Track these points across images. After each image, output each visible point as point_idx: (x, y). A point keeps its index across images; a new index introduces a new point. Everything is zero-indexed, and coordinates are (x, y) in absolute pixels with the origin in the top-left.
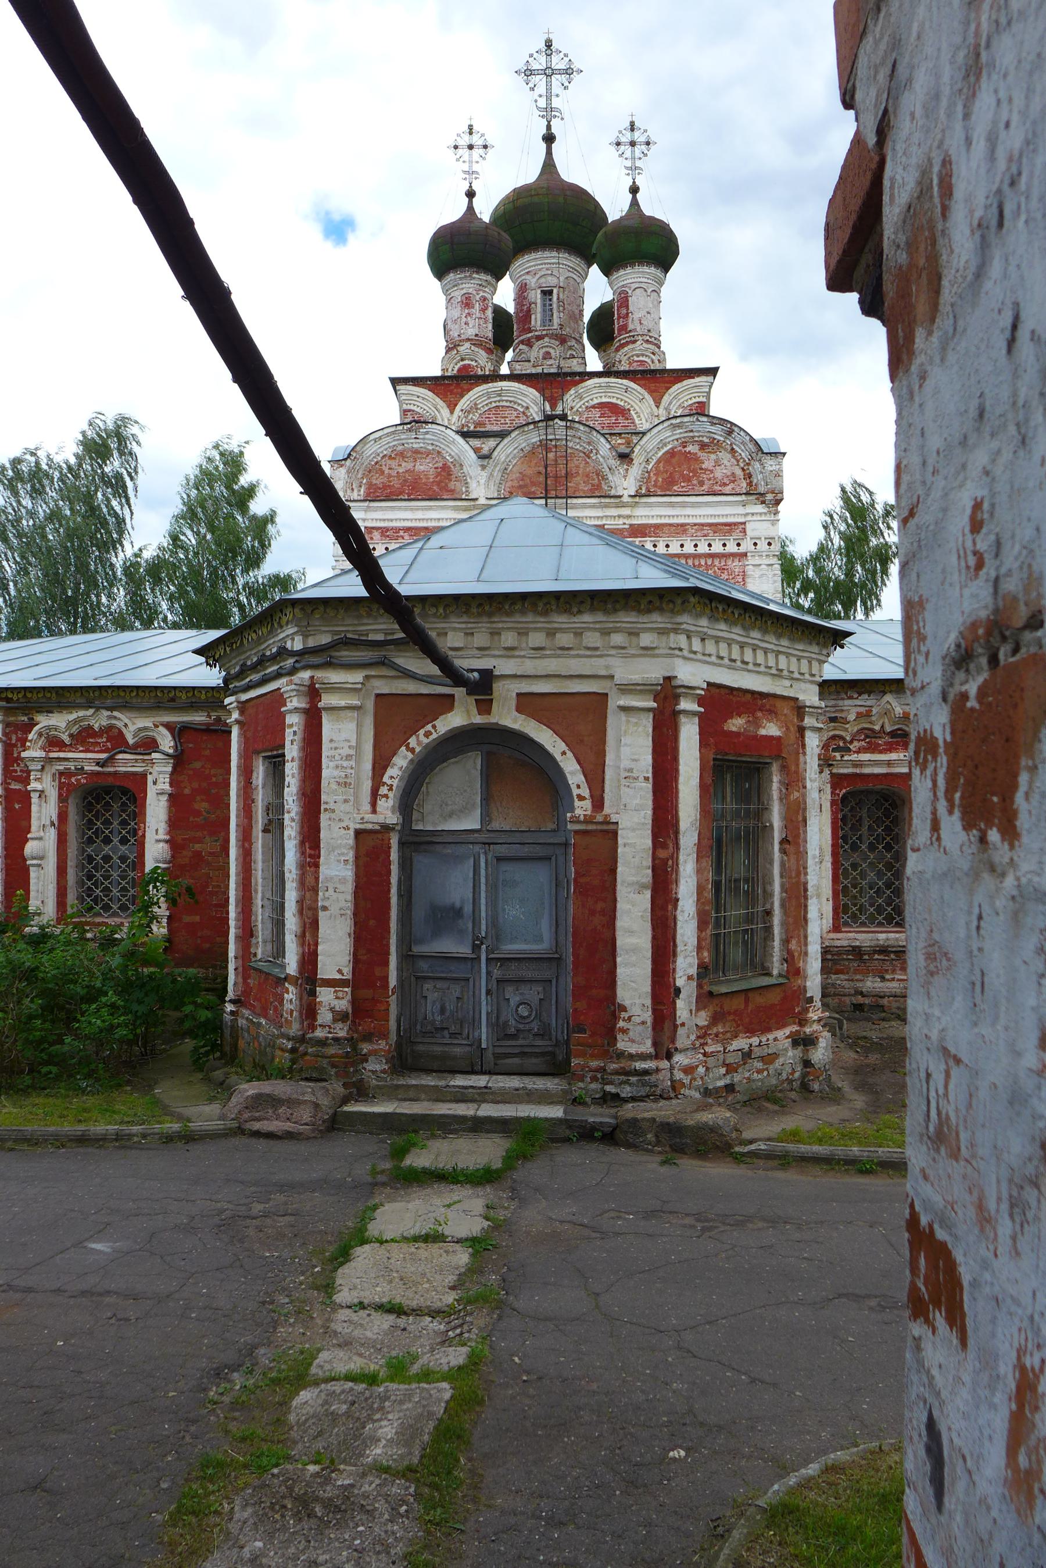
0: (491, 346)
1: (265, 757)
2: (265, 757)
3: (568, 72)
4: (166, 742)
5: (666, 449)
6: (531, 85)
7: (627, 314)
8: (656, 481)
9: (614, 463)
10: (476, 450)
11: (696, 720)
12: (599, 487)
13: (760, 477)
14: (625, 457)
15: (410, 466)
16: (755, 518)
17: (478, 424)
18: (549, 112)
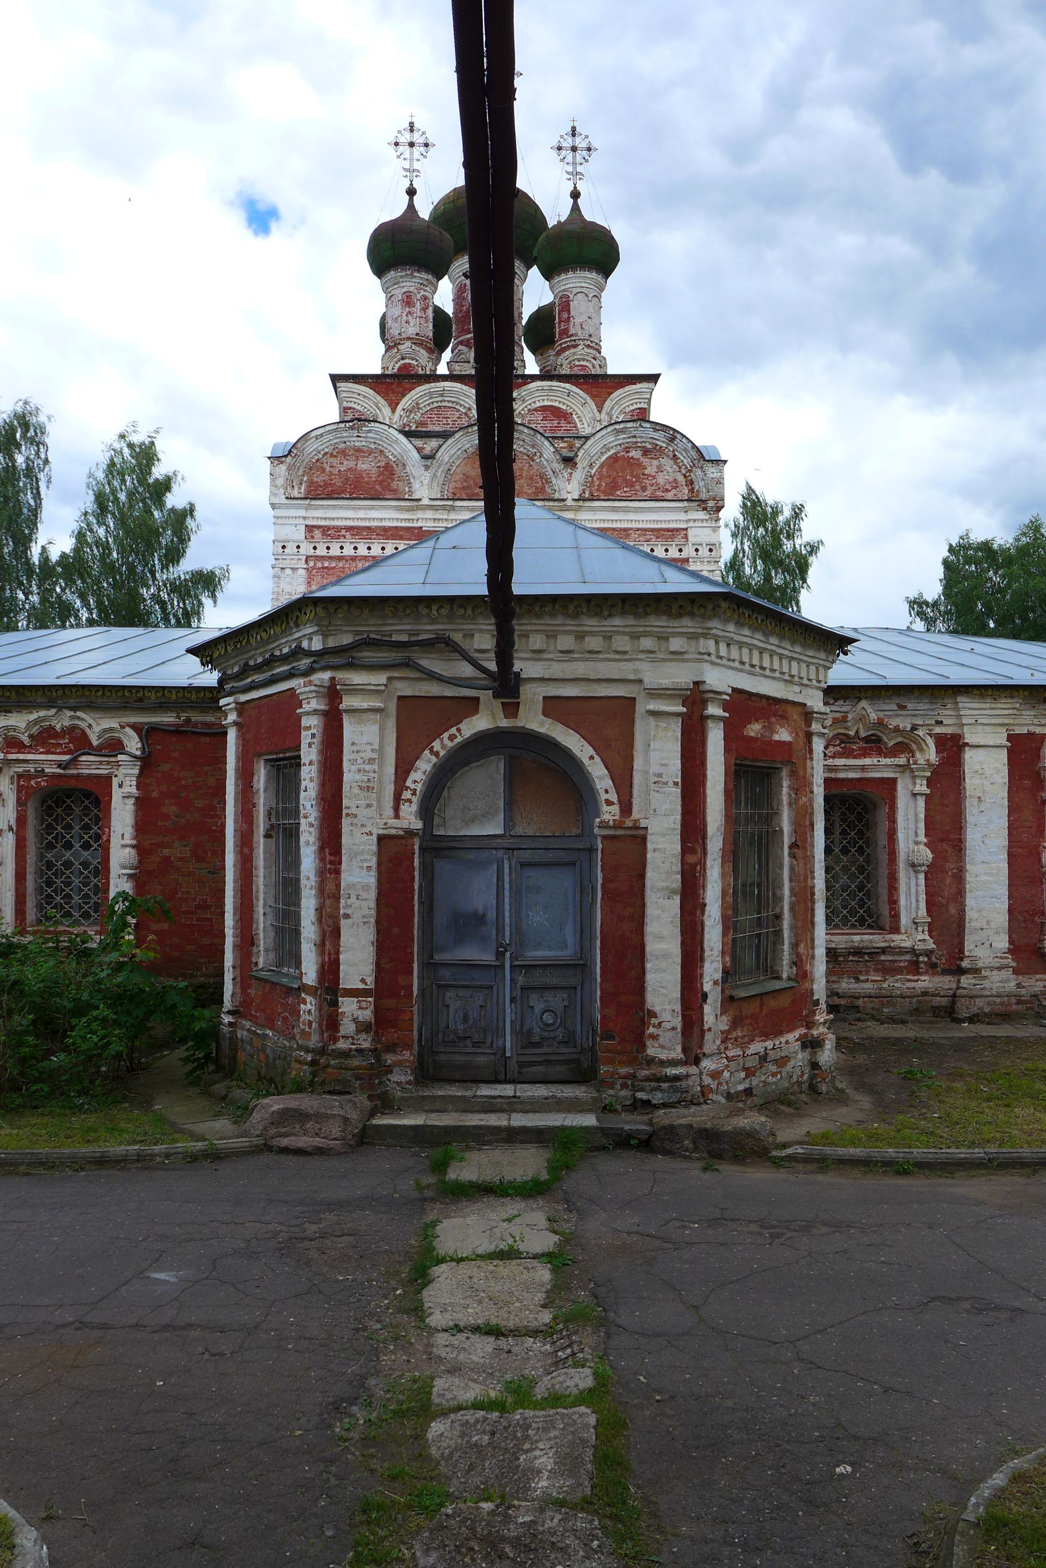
0: (432, 346)
1: (267, 760)
2: (267, 760)
4: (133, 744)
5: (609, 454)
7: (569, 318)
8: (599, 485)
9: (558, 466)
10: (419, 450)
11: (721, 725)
12: (542, 490)
13: (702, 484)
14: (569, 461)
15: (352, 464)
16: (696, 524)
17: (420, 424)
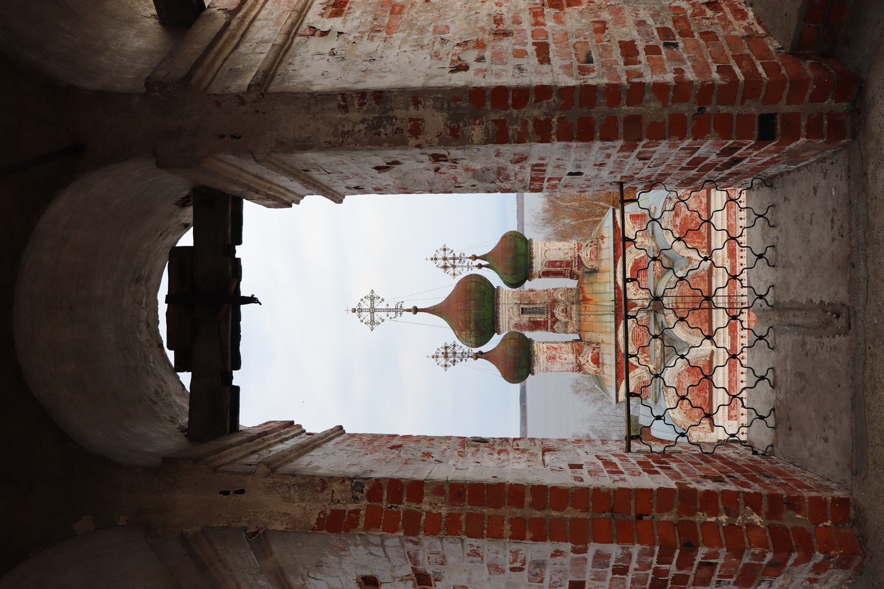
3: (372, 299)
6: (380, 321)
7: (560, 261)
8: (699, 243)
18: (399, 310)
